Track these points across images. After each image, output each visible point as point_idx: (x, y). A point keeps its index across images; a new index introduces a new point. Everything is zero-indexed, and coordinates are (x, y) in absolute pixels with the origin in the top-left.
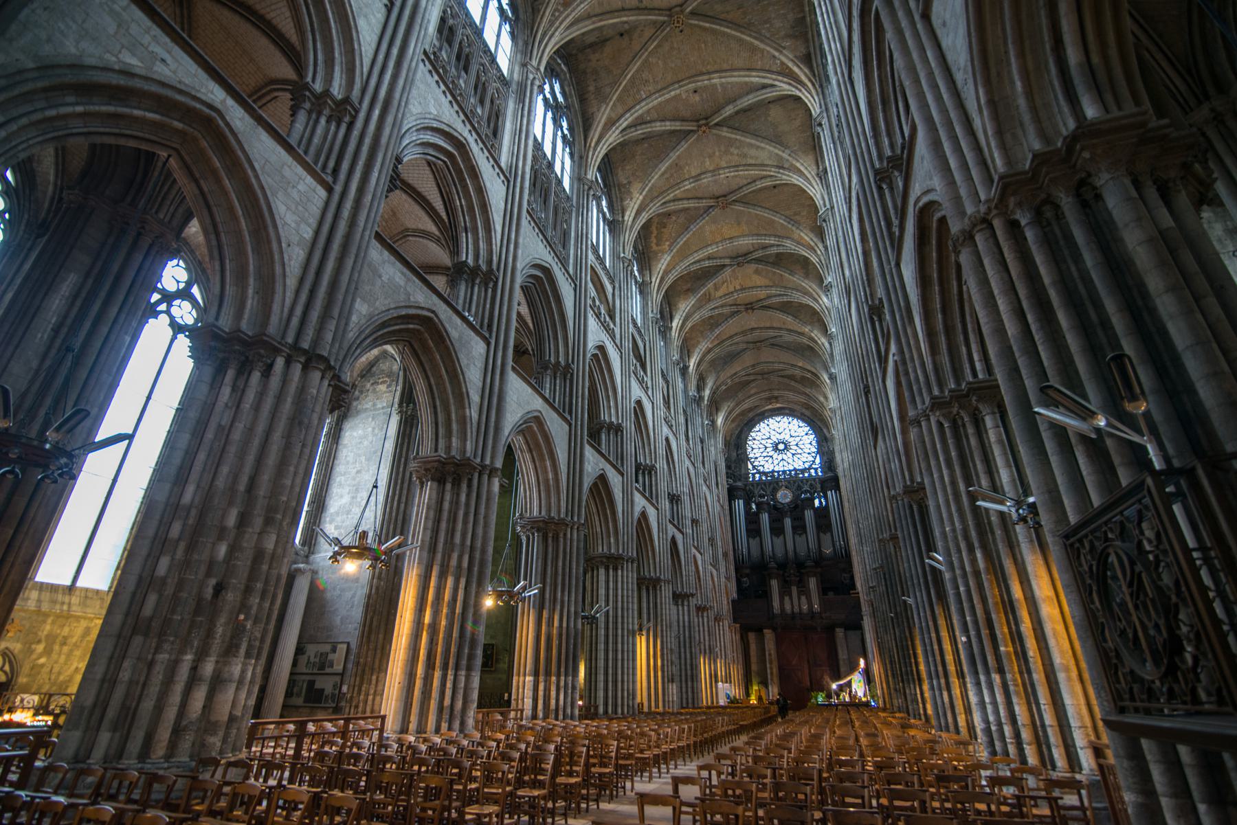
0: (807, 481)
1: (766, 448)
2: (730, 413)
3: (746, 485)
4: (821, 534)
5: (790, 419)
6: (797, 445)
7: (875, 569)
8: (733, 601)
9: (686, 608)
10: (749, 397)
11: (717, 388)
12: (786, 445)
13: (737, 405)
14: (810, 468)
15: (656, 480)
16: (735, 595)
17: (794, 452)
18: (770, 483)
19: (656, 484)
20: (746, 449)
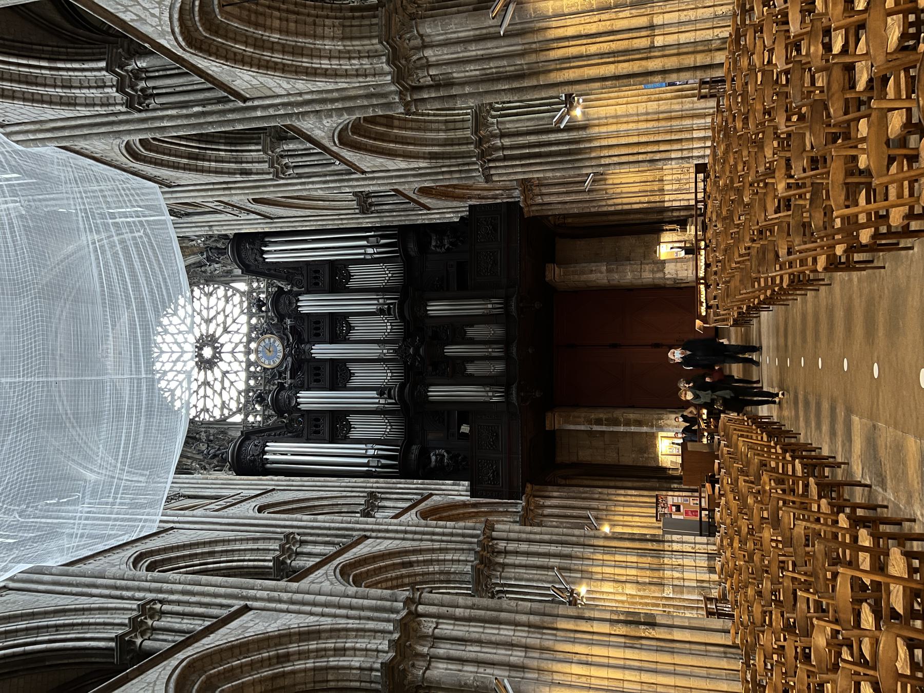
4: (351, 284)
17: (220, 330)
20: (203, 423)
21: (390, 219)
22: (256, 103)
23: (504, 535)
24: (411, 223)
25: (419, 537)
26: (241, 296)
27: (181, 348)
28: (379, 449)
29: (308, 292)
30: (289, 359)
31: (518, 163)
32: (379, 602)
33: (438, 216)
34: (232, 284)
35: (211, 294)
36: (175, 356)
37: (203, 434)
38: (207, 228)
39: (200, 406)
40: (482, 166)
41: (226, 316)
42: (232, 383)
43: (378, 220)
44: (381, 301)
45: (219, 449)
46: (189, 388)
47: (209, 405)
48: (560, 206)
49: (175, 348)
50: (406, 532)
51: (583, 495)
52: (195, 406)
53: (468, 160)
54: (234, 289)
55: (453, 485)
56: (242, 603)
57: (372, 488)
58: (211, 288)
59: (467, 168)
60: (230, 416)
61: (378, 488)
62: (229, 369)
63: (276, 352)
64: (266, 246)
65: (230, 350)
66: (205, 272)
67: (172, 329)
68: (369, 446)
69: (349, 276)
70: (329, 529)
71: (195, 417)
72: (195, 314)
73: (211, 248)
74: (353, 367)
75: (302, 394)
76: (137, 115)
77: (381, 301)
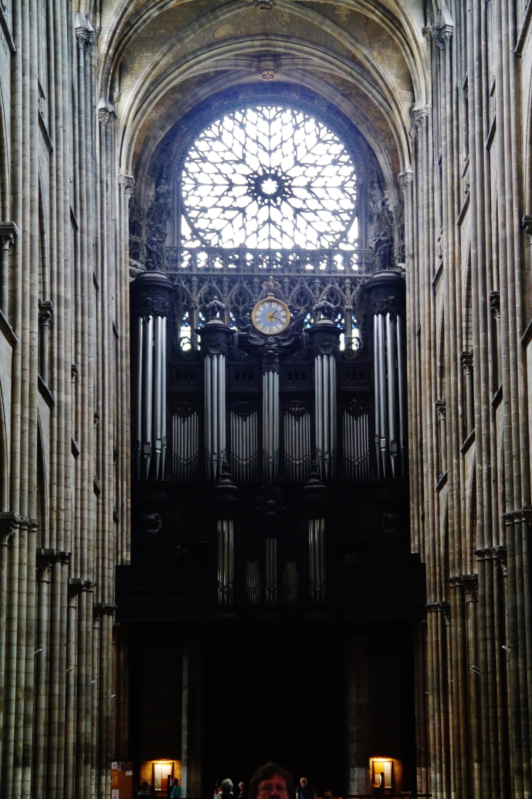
0: (324, 281)
1: (231, 185)
2: (156, 83)
3: (172, 278)
4: (348, 419)
5: (300, 117)
6: (308, 187)
7: (510, 517)
8: (120, 570)
9: (45, 588)
10: (210, 46)
11: (137, 13)
12: (280, 182)
13: (177, 62)
14: (330, 253)
15: (14, 266)
16: (127, 556)
17: (297, 203)
18: (233, 280)
19: (13, 278)
20: (179, 183)
21: (415, 472)
22: (461, 461)
23: (105, 626)
24: (411, 495)
25: (100, 546)
26: (341, 233)
27: (275, 149)
28: (161, 454)
29: (338, 366)
30: (261, 342)
31: (440, 638)
32: (86, 561)
33: (416, 527)
34: (356, 219)
35: (344, 191)
36: (263, 140)
37: (166, 187)
38: (411, 252)
39: (201, 178)
40: (438, 605)
41: (315, 212)
42: (231, 221)
43: (414, 459)
44: (327, 456)
45: (157, 256)
46: (224, 161)
47: (202, 191)
48: (421, 660)
49: (275, 142)
50: (103, 531)
51: (122, 685)
52: (201, 171)
53: (444, 593)
54: (351, 222)
55: (127, 544)
56: (79, 450)
57: (122, 453)
58: (352, 191)
59: (438, 591)
60: (188, 219)
61: (122, 459)
62: (248, 217)
63: (271, 325)
64: (390, 318)
65: (273, 219)
66: (372, 186)
67: (299, 135)
68: (165, 442)
69: (356, 415)
70: (103, 454)
71: (187, 170)
72: (319, 169)
73: (391, 246)
74: (251, 420)
75: (222, 360)
76: (459, 355)
77: (327, 456)
